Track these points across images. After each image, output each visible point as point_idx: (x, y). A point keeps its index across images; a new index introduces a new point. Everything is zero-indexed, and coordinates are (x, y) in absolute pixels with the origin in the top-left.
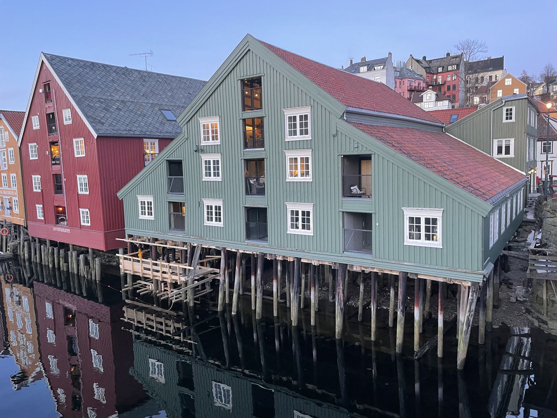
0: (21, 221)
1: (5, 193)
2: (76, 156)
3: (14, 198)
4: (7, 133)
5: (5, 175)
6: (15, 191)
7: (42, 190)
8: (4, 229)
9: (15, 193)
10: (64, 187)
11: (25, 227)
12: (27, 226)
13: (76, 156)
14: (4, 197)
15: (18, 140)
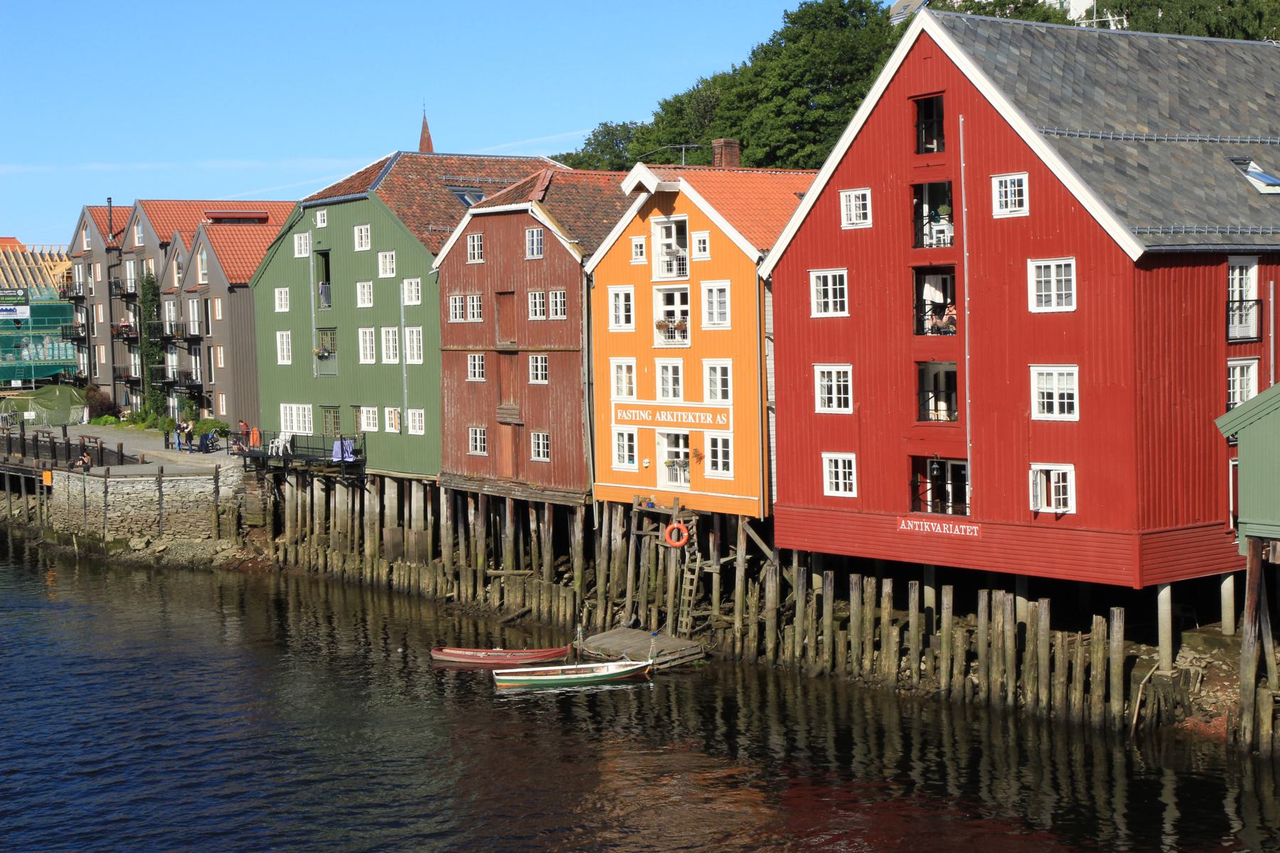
0: (748, 504)
1: (662, 417)
2: (1033, 307)
3: (709, 435)
4: (705, 235)
5: (679, 362)
6: (715, 412)
7: (858, 410)
8: (675, 525)
9: (720, 420)
10: (968, 401)
11: (753, 522)
12: (769, 520)
13: (1033, 307)
14: (659, 430)
15: (761, 259)
